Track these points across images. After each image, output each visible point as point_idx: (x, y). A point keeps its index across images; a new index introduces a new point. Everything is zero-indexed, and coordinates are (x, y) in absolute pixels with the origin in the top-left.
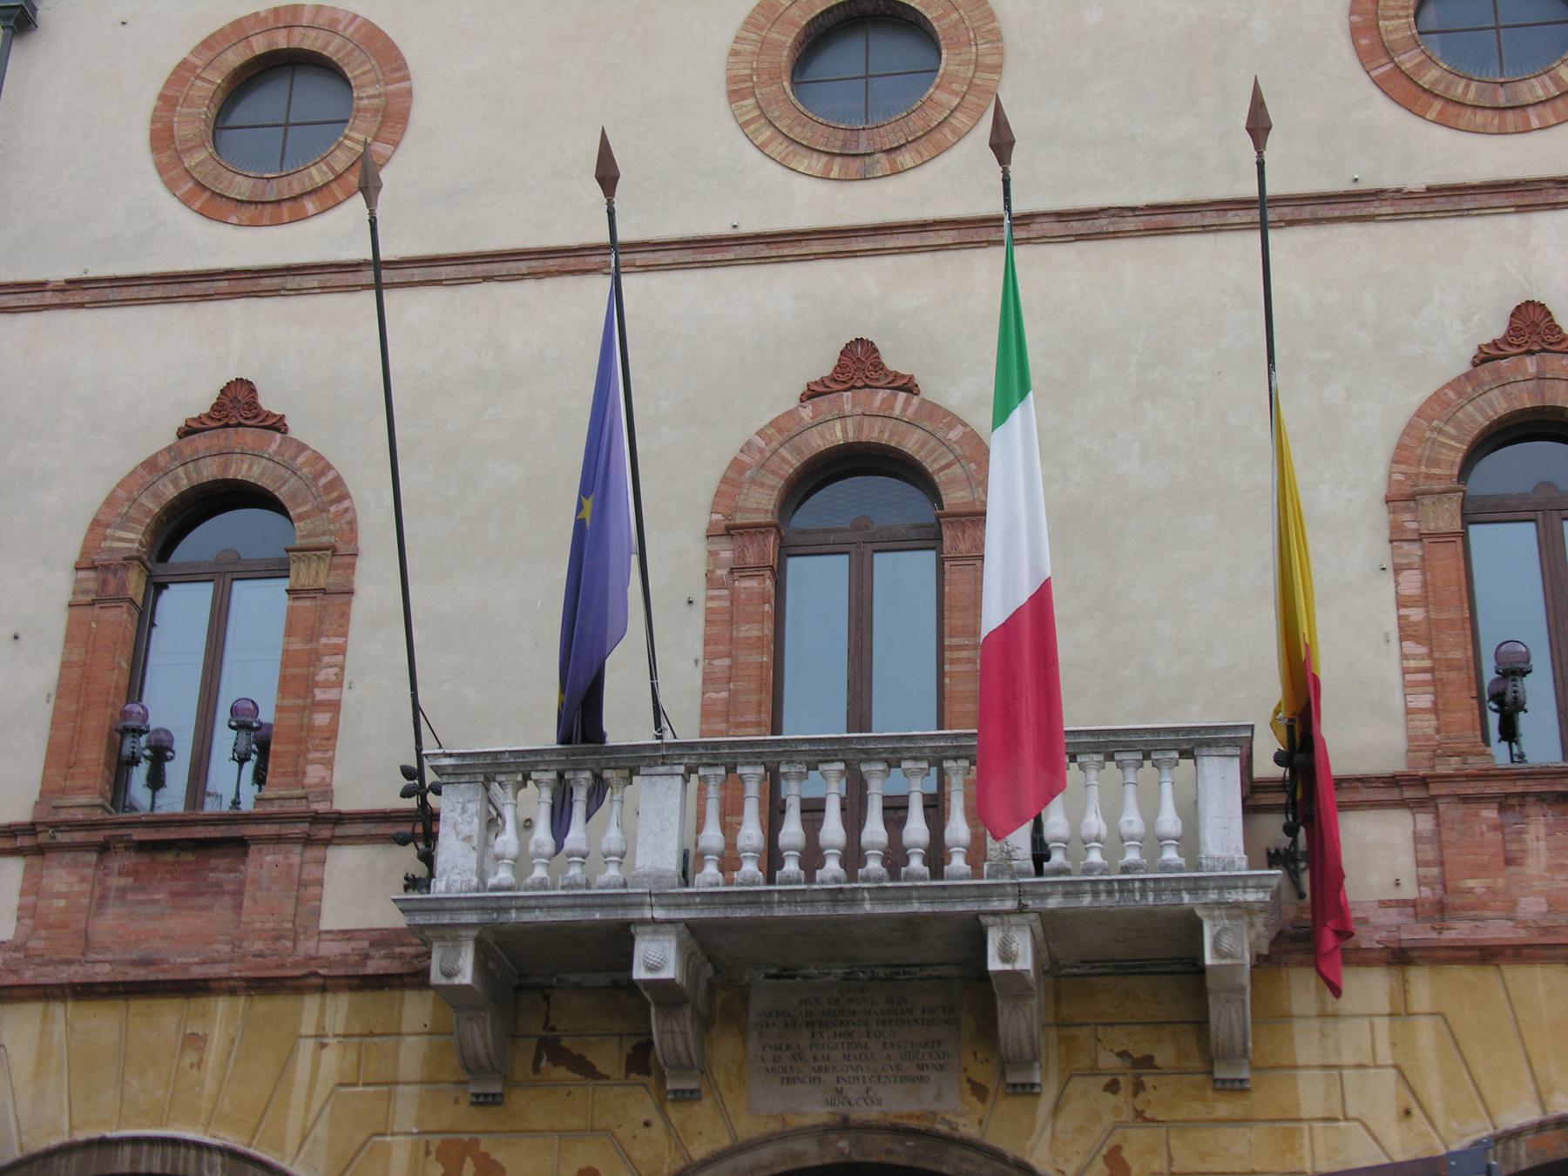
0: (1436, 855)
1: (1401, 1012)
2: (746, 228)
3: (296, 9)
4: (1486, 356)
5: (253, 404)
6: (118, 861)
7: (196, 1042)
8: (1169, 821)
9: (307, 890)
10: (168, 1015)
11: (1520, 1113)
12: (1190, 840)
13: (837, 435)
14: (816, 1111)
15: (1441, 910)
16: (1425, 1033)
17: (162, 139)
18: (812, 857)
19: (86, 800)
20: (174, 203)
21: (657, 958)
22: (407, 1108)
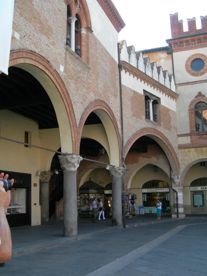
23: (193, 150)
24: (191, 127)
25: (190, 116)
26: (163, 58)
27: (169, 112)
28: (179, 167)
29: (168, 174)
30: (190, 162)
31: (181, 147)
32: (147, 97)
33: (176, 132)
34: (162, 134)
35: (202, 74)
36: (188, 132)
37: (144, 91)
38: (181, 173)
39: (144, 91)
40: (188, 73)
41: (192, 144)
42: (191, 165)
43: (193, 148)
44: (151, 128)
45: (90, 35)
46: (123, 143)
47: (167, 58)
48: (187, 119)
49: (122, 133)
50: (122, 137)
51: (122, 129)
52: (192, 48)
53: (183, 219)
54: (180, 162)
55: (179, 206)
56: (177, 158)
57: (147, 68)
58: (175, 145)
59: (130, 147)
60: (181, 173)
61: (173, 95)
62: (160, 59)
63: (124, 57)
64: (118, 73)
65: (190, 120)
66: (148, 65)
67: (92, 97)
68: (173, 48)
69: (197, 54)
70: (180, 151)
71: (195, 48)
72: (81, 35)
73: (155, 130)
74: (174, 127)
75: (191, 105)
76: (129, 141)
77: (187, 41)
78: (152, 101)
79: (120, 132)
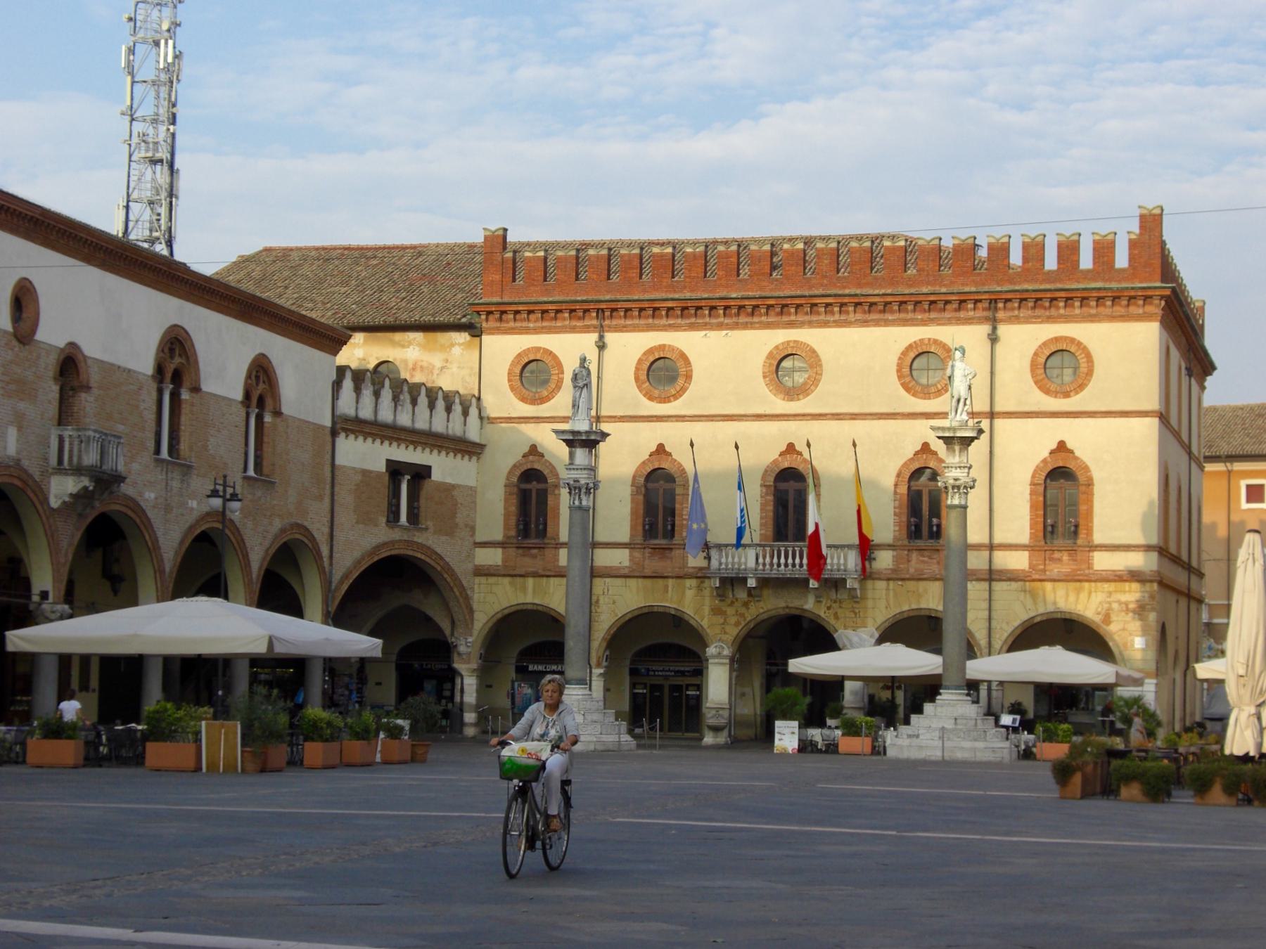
0: (896, 560)
1: (888, 589)
2: (768, 412)
3: (664, 346)
4: (917, 453)
5: (665, 451)
6: (647, 550)
7: (666, 587)
8: (842, 561)
9: (684, 558)
10: (660, 581)
11: (906, 608)
12: (845, 564)
13: (786, 465)
14: (783, 605)
15: (894, 571)
16: (891, 593)
17: (637, 379)
18: (779, 565)
19: (639, 539)
20: (641, 396)
21: (752, 583)
22: (707, 601)
23: (506, 580)
24: (506, 527)
25: (506, 500)
26: (460, 345)
27: (455, 493)
28: (472, 620)
29: (447, 632)
30: (497, 608)
31: (481, 572)
32: (395, 470)
33: (473, 535)
34: (429, 548)
35: (542, 400)
36: (498, 536)
37: (389, 462)
38: (475, 633)
39: (389, 462)
40: (512, 395)
41: (505, 566)
42: (499, 616)
43: (504, 576)
44: (400, 541)
45: (278, 420)
46: (330, 582)
47: (467, 346)
48: (499, 508)
49: (331, 564)
50: (331, 572)
51: (331, 557)
52: (527, 331)
53: (474, 738)
54: (475, 606)
55: (466, 708)
56: (467, 599)
57: (399, 408)
58: (461, 568)
59: (345, 587)
60: (475, 633)
61: (470, 449)
62: (452, 345)
63: (347, 404)
64: (329, 447)
65: (505, 509)
66: (404, 401)
67: (277, 524)
68: (484, 325)
69: (538, 349)
70: (477, 580)
71: (536, 331)
72: (263, 423)
73: (410, 543)
74: (466, 526)
75: (510, 472)
76: (346, 576)
77: (517, 312)
78: (408, 477)
79: (326, 560)
